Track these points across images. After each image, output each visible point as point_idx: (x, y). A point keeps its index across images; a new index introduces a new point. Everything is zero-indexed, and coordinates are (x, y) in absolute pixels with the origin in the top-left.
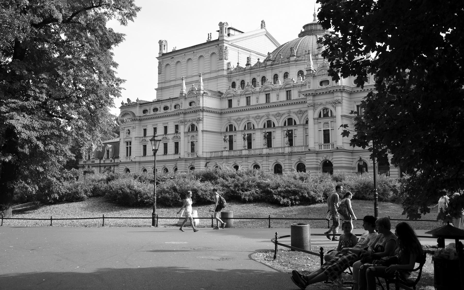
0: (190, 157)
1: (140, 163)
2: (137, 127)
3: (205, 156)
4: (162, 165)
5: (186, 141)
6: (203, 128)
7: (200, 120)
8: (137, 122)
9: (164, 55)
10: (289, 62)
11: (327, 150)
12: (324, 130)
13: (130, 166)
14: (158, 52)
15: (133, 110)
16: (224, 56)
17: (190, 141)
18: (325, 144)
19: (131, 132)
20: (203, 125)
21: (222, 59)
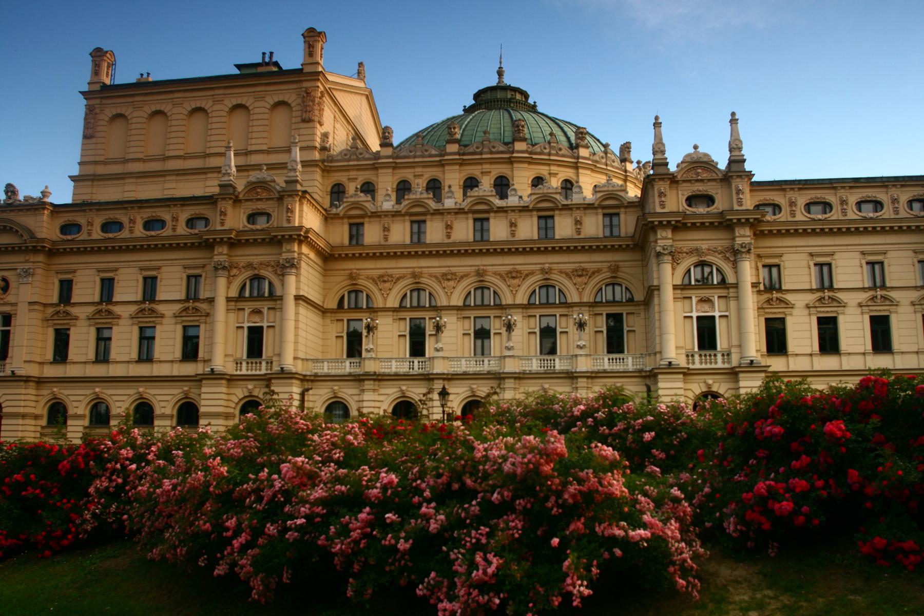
0: (244, 372)
1: (40, 382)
2: (39, 271)
3: (299, 368)
4: (88, 392)
5: (233, 324)
6: (298, 289)
7: (293, 266)
8: (41, 258)
9: (105, 87)
10: (513, 152)
11: (708, 366)
12: (698, 318)
13: (66, 392)
14: (88, 80)
15: (28, 220)
16: (317, 113)
17: (246, 325)
18: (703, 353)
19: (13, 285)
20: (298, 281)
21: (310, 121)
